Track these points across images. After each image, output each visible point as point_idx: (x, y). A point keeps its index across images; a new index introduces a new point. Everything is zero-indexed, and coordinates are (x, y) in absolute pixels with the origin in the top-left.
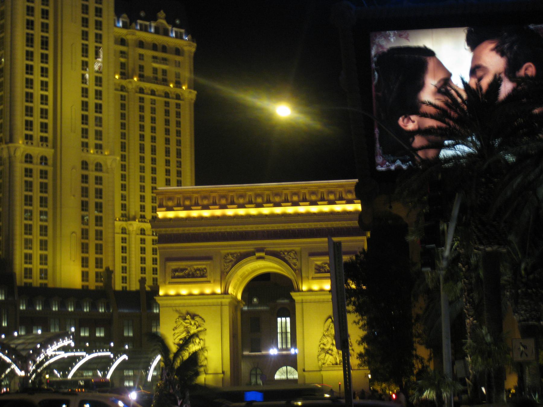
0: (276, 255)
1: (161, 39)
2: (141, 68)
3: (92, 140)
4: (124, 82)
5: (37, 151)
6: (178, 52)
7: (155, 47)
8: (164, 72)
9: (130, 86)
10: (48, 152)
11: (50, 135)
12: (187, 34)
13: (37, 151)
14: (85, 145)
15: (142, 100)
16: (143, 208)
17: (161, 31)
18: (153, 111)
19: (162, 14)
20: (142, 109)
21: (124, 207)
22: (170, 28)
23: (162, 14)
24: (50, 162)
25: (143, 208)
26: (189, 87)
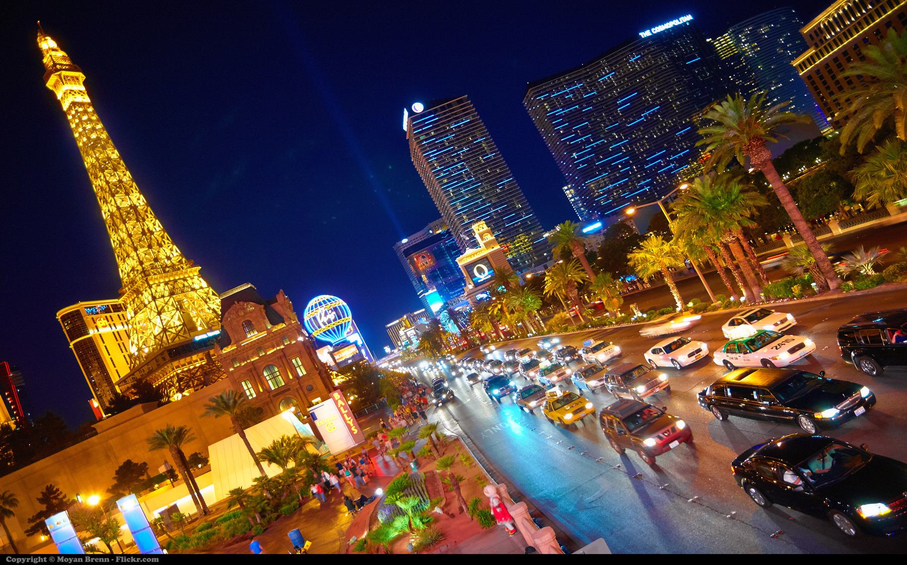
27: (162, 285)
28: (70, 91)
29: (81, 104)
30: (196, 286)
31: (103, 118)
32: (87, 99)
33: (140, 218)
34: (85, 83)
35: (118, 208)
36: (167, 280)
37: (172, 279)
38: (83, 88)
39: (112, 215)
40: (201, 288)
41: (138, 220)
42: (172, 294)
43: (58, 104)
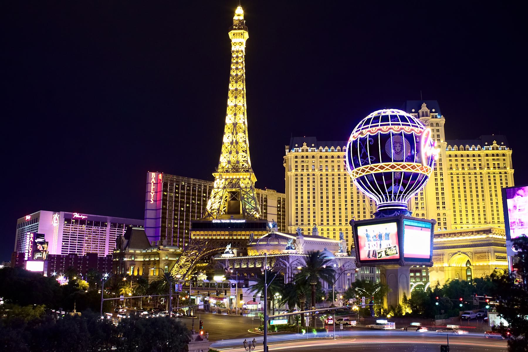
0: (464, 253)
1: (495, 152)
2: (488, 164)
3: (441, 205)
4: (481, 171)
6: (504, 155)
7: (493, 155)
8: (498, 164)
9: (483, 172)
11: (425, 206)
12: (507, 147)
14: (438, 208)
15: (489, 176)
16: (493, 218)
17: (495, 148)
18: (495, 180)
19: (495, 142)
20: (489, 180)
21: (485, 219)
22: (499, 146)
23: (495, 142)
24: (425, 215)
25: (493, 218)
26: (511, 168)
27: (223, 180)
30: (242, 185)
36: (228, 177)
37: (231, 177)
41: (233, 134)
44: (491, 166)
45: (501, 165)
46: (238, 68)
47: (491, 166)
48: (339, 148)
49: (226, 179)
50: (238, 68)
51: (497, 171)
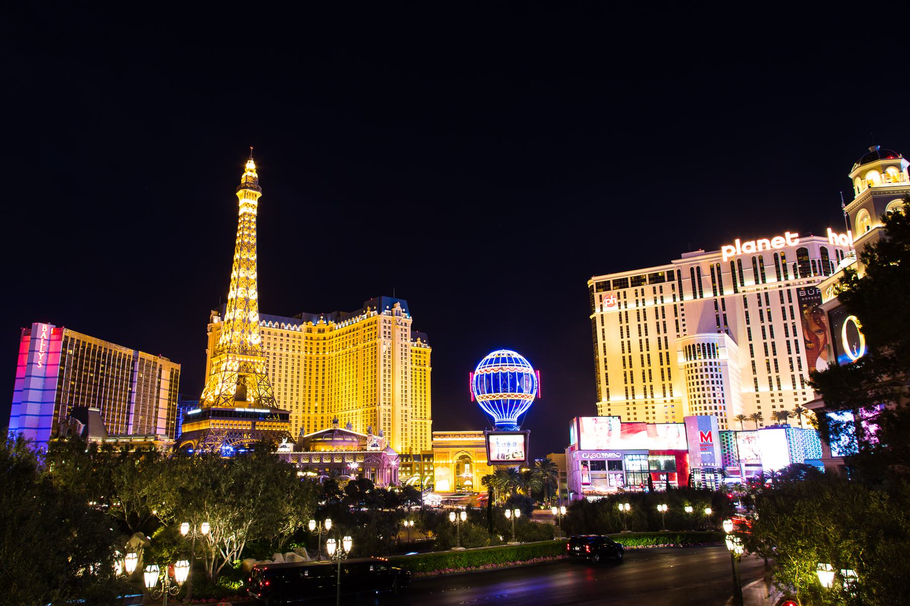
1: (418, 349)
5: (387, 407)
10: (390, 408)
13: (387, 407)
19: (419, 339)
23: (419, 339)
28: (248, 203)
29: (250, 215)
30: (258, 371)
31: (258, 229)
32: (255, 212)
33: (247, 309)
34: (260, 200)
35: (237, 298)
38: (256, 203)
39: (232, 300)
40: (261, 373)
42: (239, 371)
43: (238, 209)
44: (414, 362)
45: (422, 363)
46: (247, 234)
47: (414, 362)
48: (277, 323)
49: (240, 362)
50: (247, 234)
51: (418, 368)
